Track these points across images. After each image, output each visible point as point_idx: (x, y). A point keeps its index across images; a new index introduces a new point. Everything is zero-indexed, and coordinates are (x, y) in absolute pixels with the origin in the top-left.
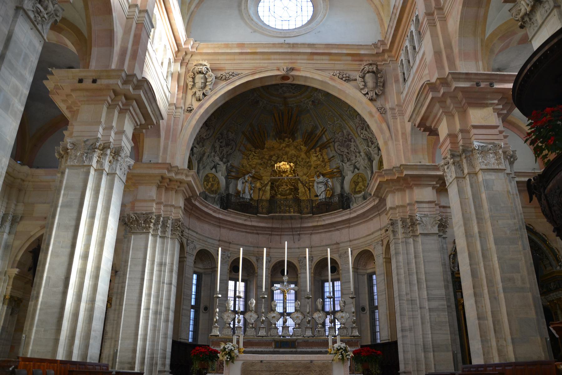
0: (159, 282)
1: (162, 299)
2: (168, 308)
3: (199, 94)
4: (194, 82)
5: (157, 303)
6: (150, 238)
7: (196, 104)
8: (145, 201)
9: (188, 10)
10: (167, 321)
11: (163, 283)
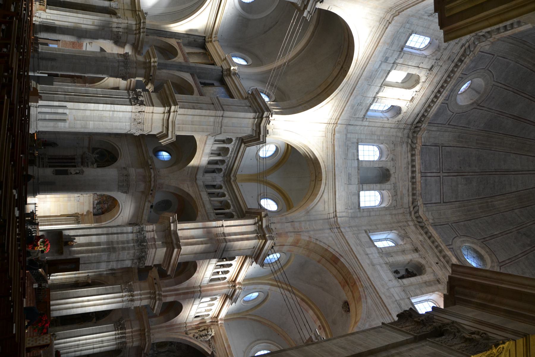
0: (93, 343)
1: (85, 346)
2: (81, 350)
3: (197, 335)
4: (202, 330)
5: (83, 345)
6: (114, 333)
7: (191, 335)
8: (131, 325)
9: (245, 315)
10: (75, 351)
11: (93, 345)
